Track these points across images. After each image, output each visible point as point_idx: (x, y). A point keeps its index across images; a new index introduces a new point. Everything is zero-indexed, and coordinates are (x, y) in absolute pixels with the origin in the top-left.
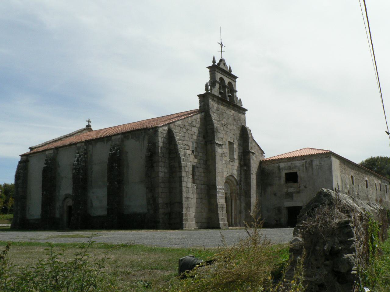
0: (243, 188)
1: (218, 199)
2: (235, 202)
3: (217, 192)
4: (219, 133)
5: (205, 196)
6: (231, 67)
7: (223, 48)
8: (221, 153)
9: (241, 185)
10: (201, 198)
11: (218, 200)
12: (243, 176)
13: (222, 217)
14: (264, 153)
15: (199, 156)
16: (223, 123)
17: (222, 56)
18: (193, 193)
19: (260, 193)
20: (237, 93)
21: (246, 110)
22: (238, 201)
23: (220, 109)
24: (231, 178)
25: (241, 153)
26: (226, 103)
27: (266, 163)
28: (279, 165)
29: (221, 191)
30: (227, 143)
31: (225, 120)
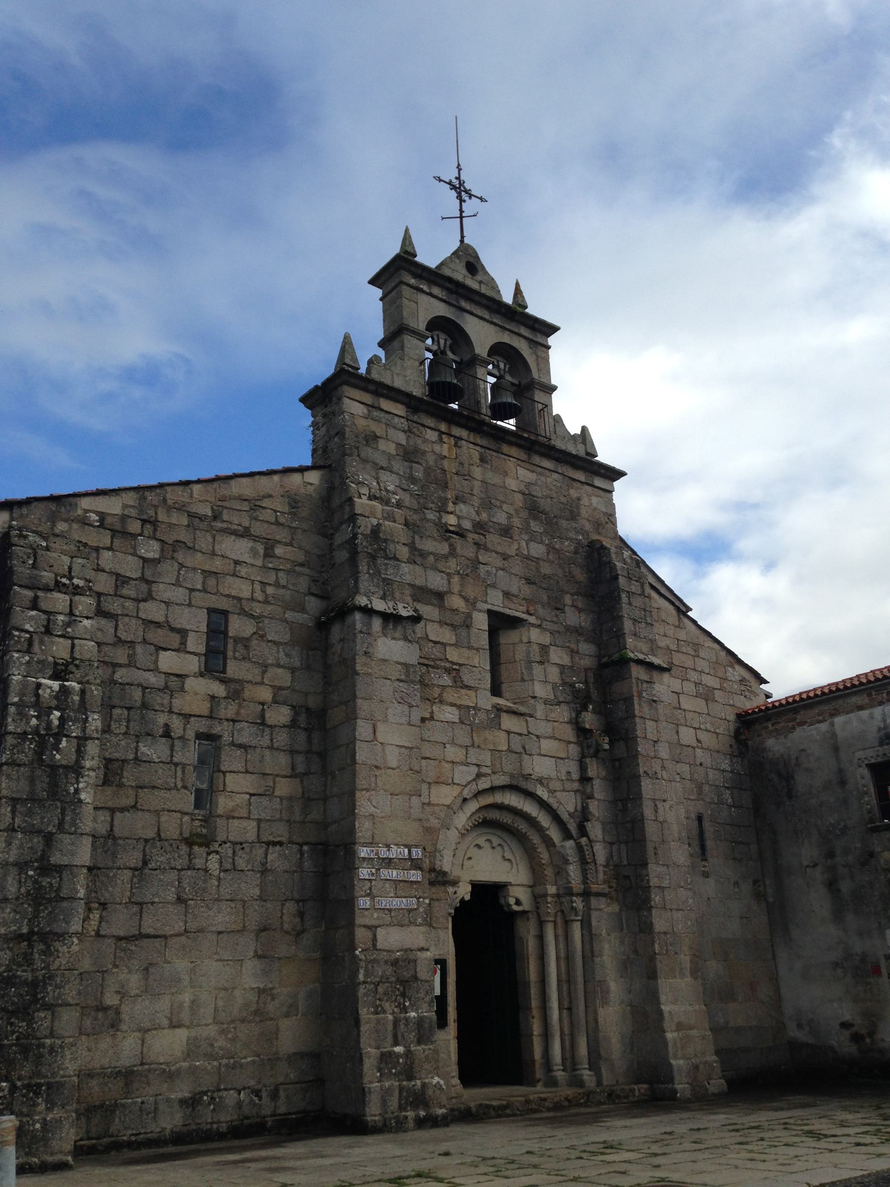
0: (600, 852)
1: (373, 928)
2: (560, 931)
3: (360, 889)
4: (391, 562)
5: (301, 914)
6: (522, 288)
7: (470, 206)
8: (406, 665)
9: (584, 840)
10: (264, 929)
11: (361, 934)
12: (599, 789)
13: (396, 1044)
14: (766, 682)
15: (262, 683)
16: (452, 520)
17: (462, 237)
18: (180, 900)
19: (755, 882)
20: (555, 396)
21: (615, 474)
22: (576, 931)
23: (431, 459)
24: (513, 800)
25: (586, 670)
26: (470, 429)
27: (770, 725)
28: (832, 724)
29: (394, 874)
30: (481, 621)
31: (462, 508)
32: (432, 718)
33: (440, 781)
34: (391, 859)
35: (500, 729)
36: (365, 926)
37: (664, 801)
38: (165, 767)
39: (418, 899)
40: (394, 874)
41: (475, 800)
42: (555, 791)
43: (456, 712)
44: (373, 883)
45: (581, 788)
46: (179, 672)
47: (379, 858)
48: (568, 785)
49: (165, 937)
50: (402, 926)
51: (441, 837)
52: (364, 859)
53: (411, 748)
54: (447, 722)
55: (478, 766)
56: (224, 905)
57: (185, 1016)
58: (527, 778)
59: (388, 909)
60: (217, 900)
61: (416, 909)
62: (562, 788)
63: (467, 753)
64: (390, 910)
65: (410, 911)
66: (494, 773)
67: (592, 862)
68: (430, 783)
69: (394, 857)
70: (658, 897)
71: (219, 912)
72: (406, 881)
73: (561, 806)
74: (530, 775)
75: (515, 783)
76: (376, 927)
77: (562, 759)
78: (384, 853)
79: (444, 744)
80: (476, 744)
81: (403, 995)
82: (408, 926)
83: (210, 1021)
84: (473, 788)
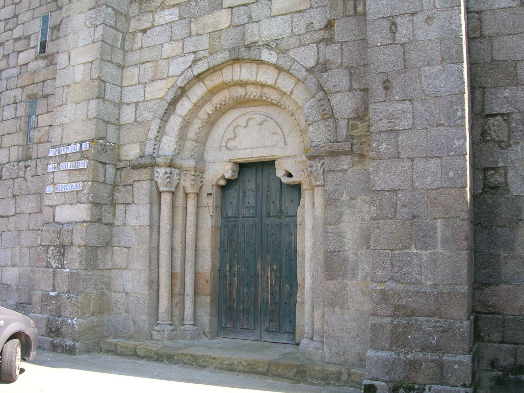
1: (53, 207)
13: (54, 290)
18: (14, 196)
29: (69, 165)
32: (153, 26)
33: (155, 78)
34: (67, 154)
35: (222, 8)
36: (49, 206)
37: (413, 14)
38: (14, 120)
39: (83, 182)
40: (69, 165)
41: (203, 85)
42: (288, 50)
43: (176, 10)
44: (55, 173)
45: (327, 36)
46: (26, 63)
47: (60, 155)
48: (307, 39)
49: (8, 217)
50: (71, 204)
51: (152, 126)
52: (51, 157)
53: (92, 62)
54: (167, 24)
55: (194, 52)
56: (31, 197)
57: (17, 260)
58: (249, 47)
59: (63, 193)
60: (29, 194)
61: (81, 191)
62: (297, 44)
63: (183, 45)
64: (64, 193)
65: (78, 192)
66: (212, 54)
67: (330, 117)
68: (146, 83)
69: (70, 152)
70: (384, 145)
71: (29, 202)
72: (76, 170)
73: (296, 64)
74: (257, 42)
75: (235, 56)
76: (55, 206)
77: (300, 11)
78: (64, 150)
79: (162, 44)
80: (194, 33)
81: (63, 255)
82: (76, 203)
83: (28, 264)
84: (190, 74)
